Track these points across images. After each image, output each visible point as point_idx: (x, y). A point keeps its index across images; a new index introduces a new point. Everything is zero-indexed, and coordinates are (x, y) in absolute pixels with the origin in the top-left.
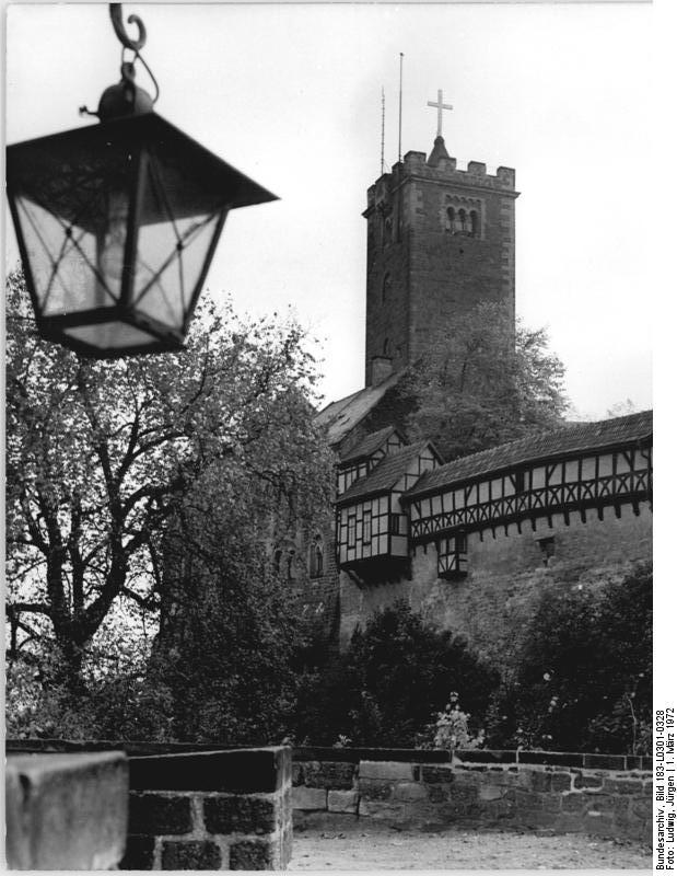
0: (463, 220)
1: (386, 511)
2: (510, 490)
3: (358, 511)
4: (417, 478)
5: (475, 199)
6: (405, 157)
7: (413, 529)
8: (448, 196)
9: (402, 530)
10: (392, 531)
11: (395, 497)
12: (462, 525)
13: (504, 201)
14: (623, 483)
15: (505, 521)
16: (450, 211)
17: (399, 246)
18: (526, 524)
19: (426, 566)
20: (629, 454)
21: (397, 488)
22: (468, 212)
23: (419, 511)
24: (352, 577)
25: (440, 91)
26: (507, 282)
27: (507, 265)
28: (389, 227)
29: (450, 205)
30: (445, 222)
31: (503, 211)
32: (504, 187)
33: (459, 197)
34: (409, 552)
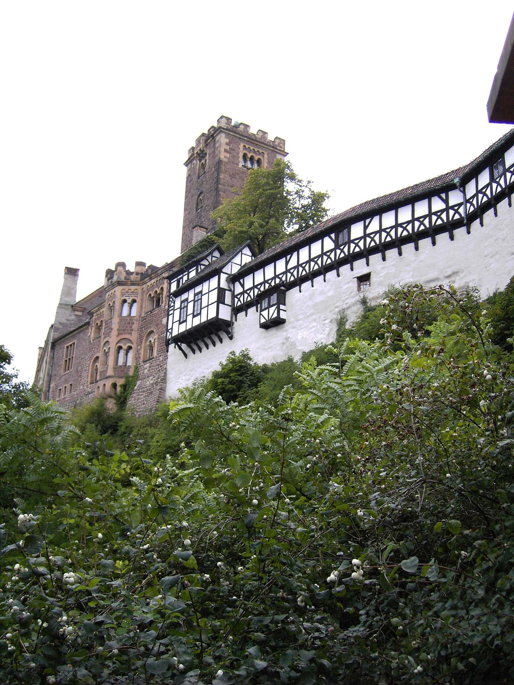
0: (252, 164)
3: (190, 295)
4: (240, 267)
5: (261, 151)
7: (236, 300)
10: (221, 300)
11: (223, 277)
14: (439, 217)
15: (324, 270)
16: (245, 156)
18: (345, 269)
19: (248, 325)
20: (443, 196)
21: (224, 270)
22: (256, 158)
23: (243, 286)
24: (180, 349)
30: (241, 159)
33: (252, 148)
34: (232, 318)
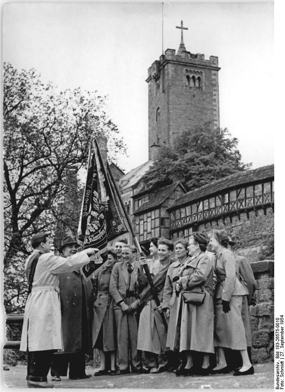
1: (157, 216)
2: (219, 203)
5: (199, 71)
6: (165, 52)
8: (187, 70)
9: (167, 224)
12: (196, 222)
13: (213, 72)
16: (188, 77)
17: (163, 94)
22: (196, 77)
25: (182, 22)
26: (215, 110)
27: (215, 102)
28: (158, 86)
29: (187, 74)
31: (213, 77)
32: (213, 65)
